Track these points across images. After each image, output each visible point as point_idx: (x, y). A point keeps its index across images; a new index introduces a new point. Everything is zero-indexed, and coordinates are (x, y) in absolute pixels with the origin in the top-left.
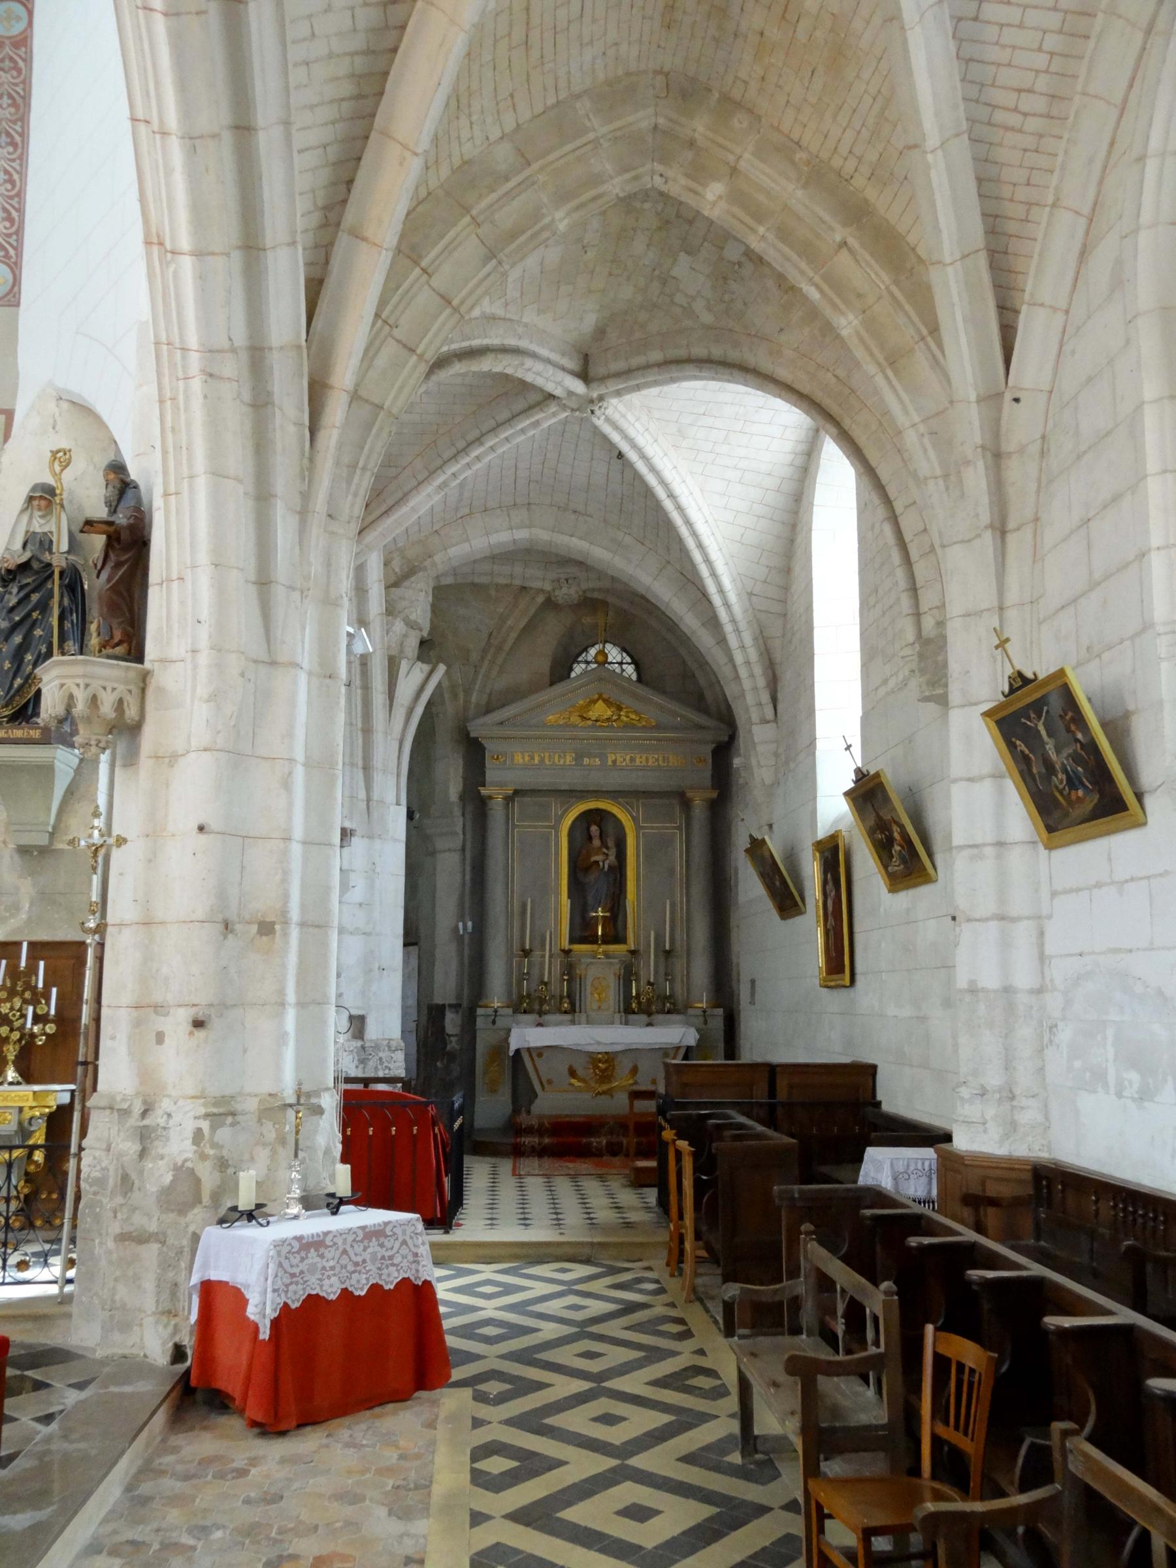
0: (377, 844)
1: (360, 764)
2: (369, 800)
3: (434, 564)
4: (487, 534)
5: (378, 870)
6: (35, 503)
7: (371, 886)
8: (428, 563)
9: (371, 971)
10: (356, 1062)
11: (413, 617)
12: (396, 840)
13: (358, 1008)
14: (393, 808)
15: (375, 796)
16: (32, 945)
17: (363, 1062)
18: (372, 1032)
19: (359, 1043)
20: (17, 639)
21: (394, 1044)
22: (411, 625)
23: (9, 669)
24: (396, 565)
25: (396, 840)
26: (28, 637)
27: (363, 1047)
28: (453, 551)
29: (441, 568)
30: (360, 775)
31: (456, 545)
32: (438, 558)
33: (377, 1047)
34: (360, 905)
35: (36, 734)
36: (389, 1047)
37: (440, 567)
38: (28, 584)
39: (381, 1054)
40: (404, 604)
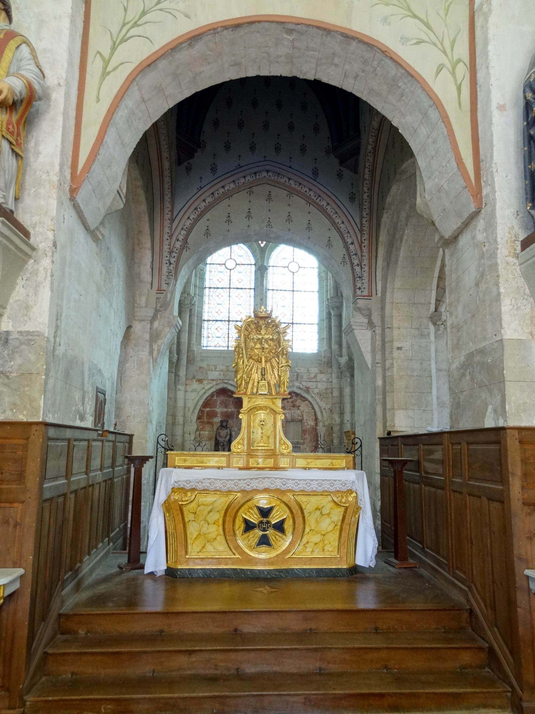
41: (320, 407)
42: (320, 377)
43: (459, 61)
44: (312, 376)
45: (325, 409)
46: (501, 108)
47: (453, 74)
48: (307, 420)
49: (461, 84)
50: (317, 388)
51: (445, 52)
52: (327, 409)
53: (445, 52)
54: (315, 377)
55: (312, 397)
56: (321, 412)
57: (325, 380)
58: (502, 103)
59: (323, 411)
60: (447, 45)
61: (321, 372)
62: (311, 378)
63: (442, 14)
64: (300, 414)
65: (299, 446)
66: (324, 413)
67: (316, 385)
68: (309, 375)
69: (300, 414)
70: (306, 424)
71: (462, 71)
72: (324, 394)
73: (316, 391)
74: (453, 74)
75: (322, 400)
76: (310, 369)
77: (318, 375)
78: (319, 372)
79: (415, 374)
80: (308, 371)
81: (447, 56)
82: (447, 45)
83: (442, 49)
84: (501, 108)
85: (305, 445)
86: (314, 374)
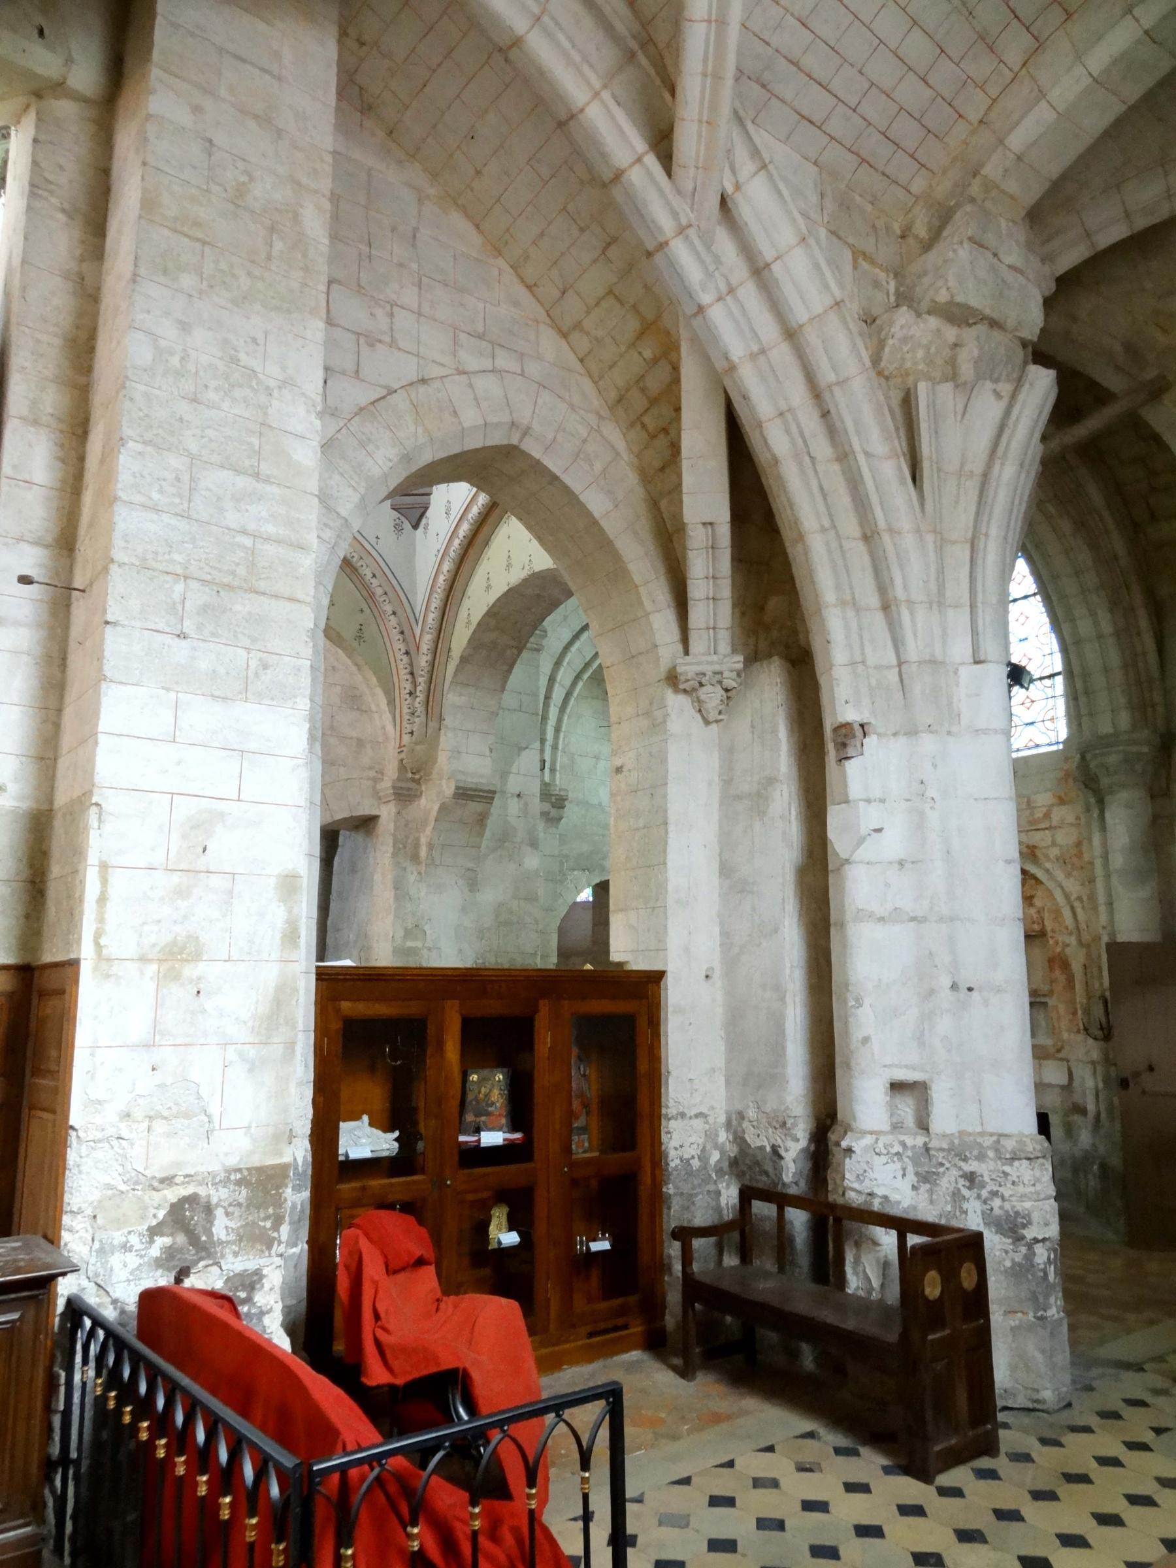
0: (928, 744)
1: (874, 601)
2: (900, 665)
3: (989, 186)
4: (1079, 56)
5: (931, 792)
7: (919, 824)
8: (975, 189)
9: (931, 992)
10: (911, 1178)
11: (943, 297)
12: (985, 731)
13: (913, 1068)
14: (967, 672)
15: (913, 650)
16: (317, 961)
17: (927, 1178)
18: (946, 1118)
19: (920, 1140)
21: (1009, 1145)
22: (958, 315)
24: (921, 229)
25: (985, 731)
27: (927, 1150)
28: (1017, 140)
29: (1029, 192)
30: (879, 618)
31: (1018, 123)
32: (991, 170)
33: (959, 1150)
34: (901, 863)
36: (997, 1151)
37: (1012, 186)
39: (970, 1167)
40: (926, 281)
41: (1067, 896)
42: (1058, 814)
44: (1039, 814)
45: (1080, 899)
48: (1053, 931)
50: (1054, 844)
52: (1085, 898)
54: (1047, 816)
55: (1047, 871)
56: (1073, 909)
57: (1070, 819)
59: (1077, 904)
61: (1062, 801)
62: (1036, 822)
64: (1035, 916)
65: (1043, 1000)
66: (1079, 911)
67: (1053, 837)
68: (1032, 814)
69: (1035, 916)
70: (1051, 942)
72: (1075, 860)
73: (1054, 852)
75: (1068, 875)
76: (1033, 797)
77: (1055, 810)
78: (1056, 801)
79: (641, 823)
80: (1029, 802)
85: (1054, 998)
86: (1044, 810)
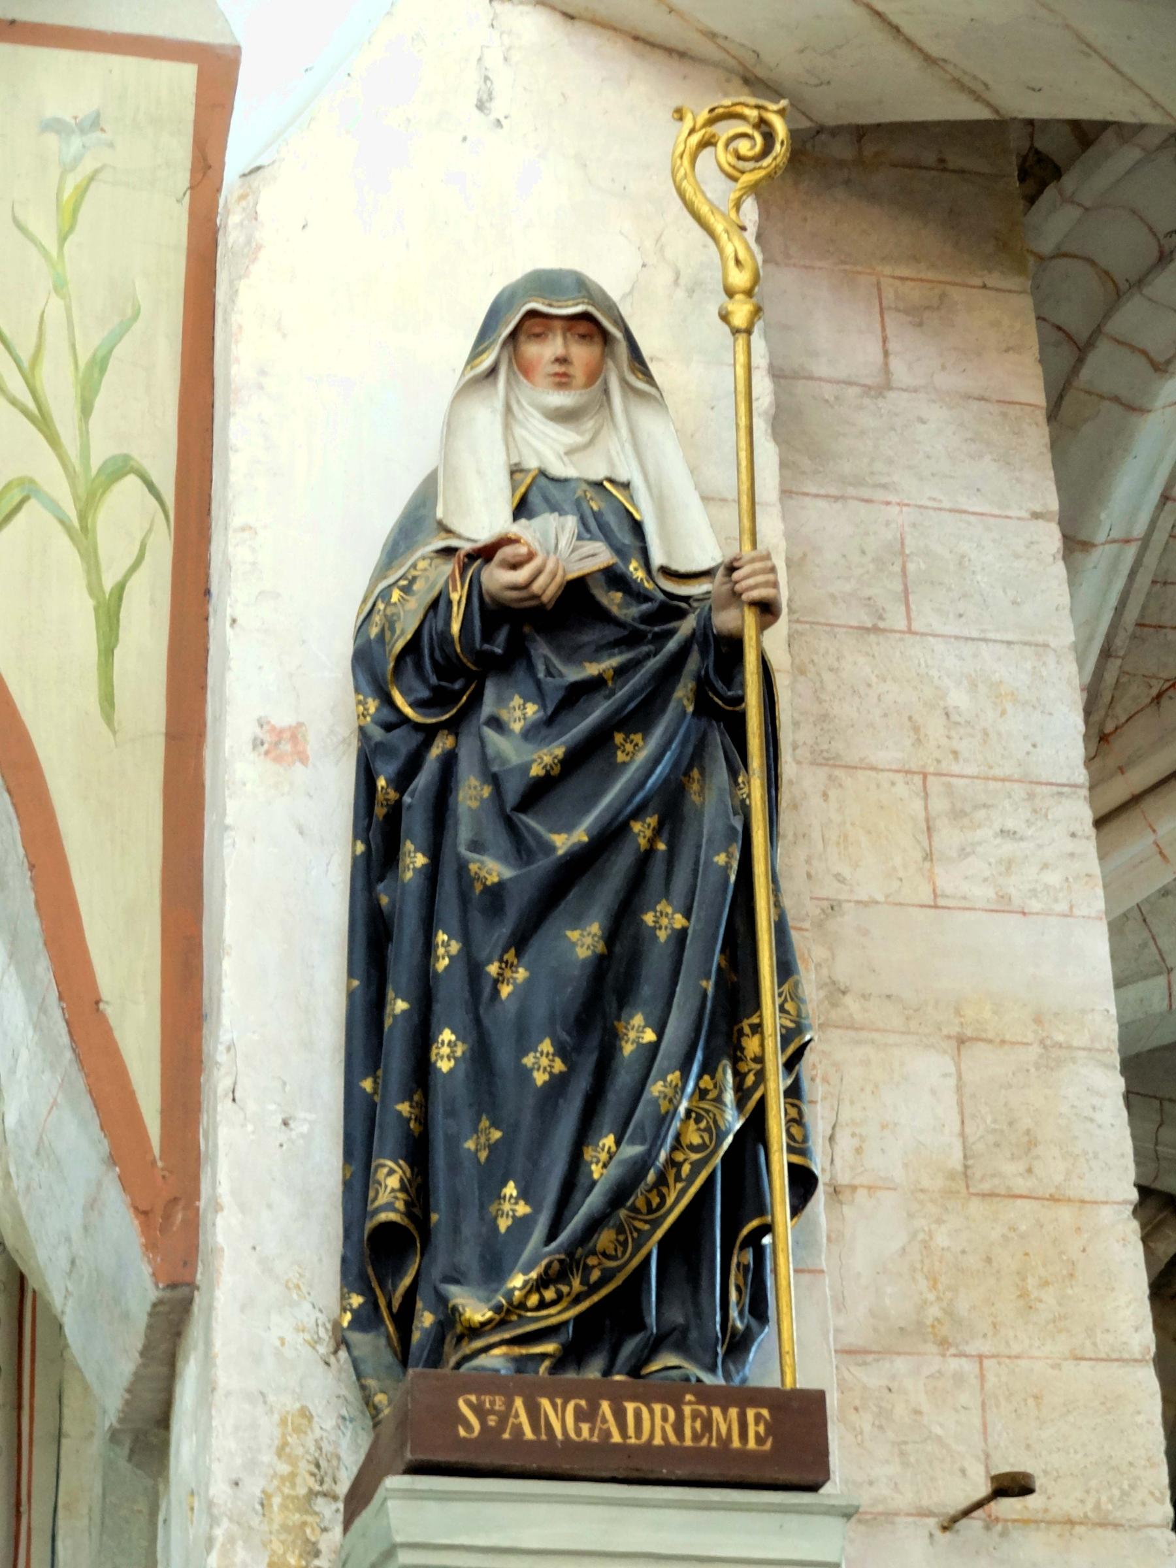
6: (545, 351)
20: (584, 940)
23: (558, 1084)
26: (623, 923)
35: (750, 1431)
38: (595, 685)
43: (120, 468)
46: (281, 744)
47: (82, 534)
49: (121, 588)
51: (42, 421)
53: (42, 421)
58: (283, 719)
60: (59, 385)
63: (43, 227)
71: (134, 524)
74: (82, 534)
81: (53, 440)
82: (59, 385)
83: (31, 405)
84: (281, 744)
